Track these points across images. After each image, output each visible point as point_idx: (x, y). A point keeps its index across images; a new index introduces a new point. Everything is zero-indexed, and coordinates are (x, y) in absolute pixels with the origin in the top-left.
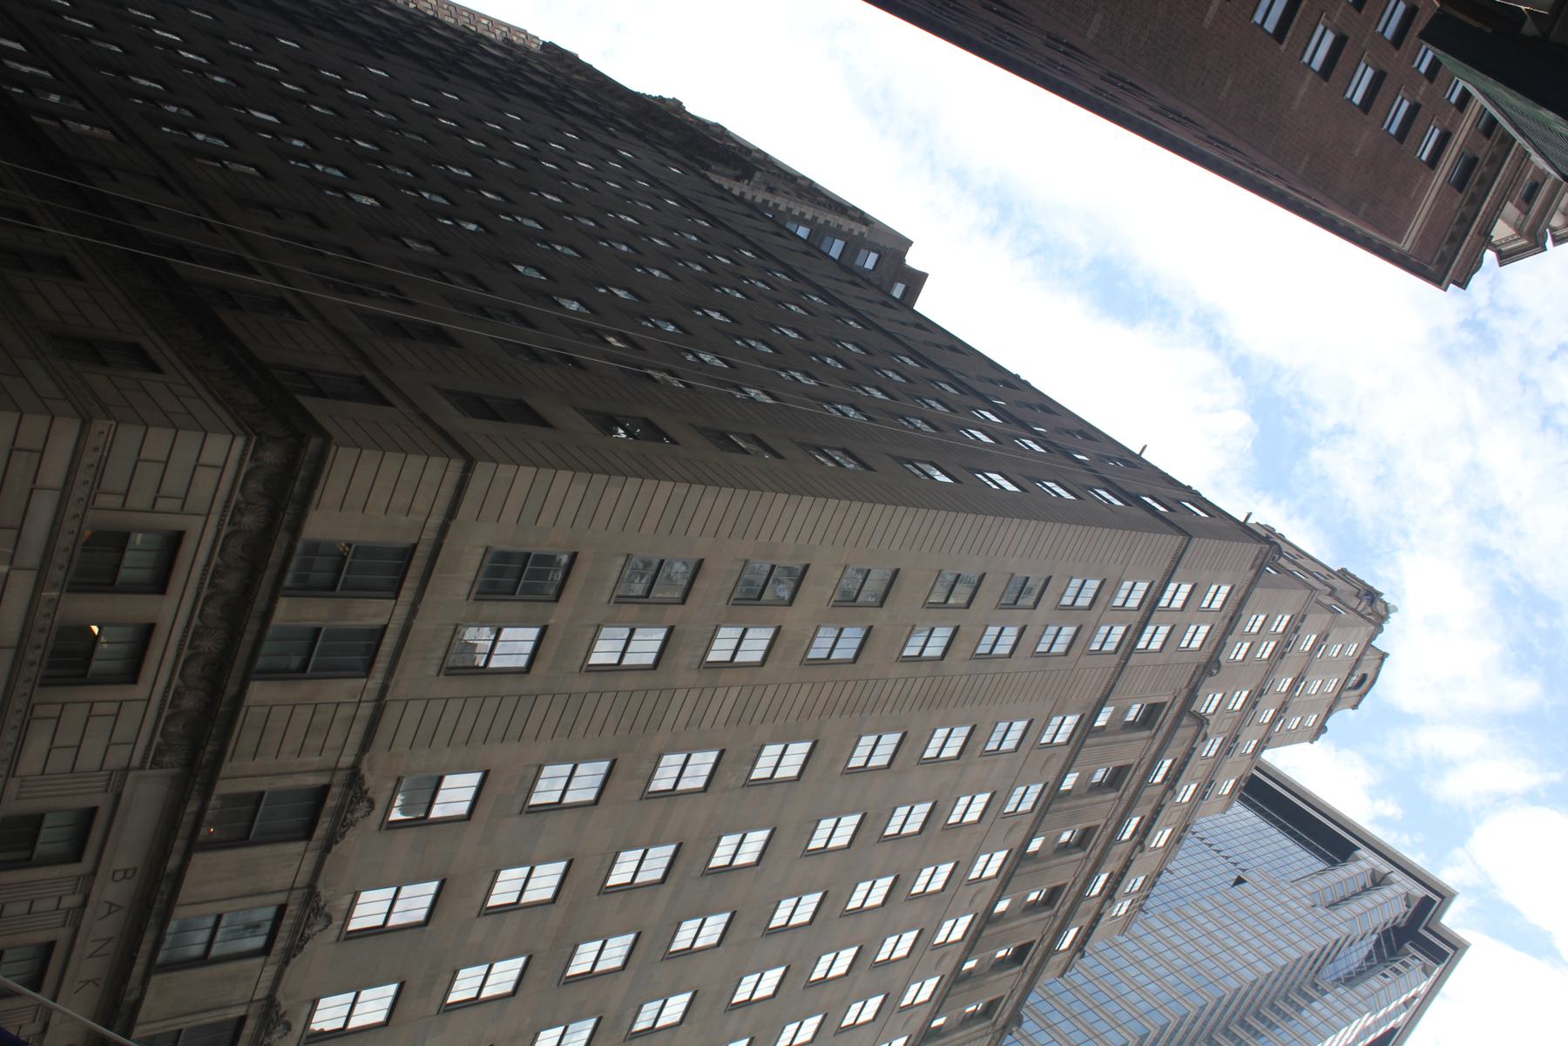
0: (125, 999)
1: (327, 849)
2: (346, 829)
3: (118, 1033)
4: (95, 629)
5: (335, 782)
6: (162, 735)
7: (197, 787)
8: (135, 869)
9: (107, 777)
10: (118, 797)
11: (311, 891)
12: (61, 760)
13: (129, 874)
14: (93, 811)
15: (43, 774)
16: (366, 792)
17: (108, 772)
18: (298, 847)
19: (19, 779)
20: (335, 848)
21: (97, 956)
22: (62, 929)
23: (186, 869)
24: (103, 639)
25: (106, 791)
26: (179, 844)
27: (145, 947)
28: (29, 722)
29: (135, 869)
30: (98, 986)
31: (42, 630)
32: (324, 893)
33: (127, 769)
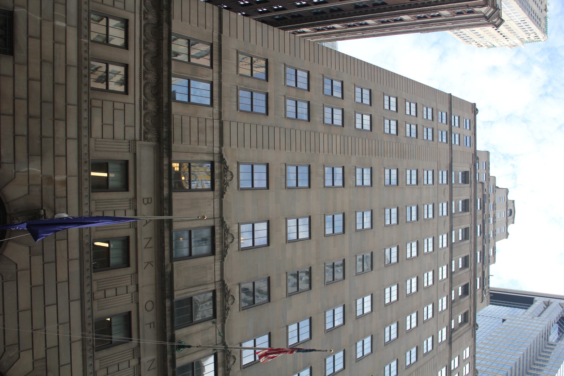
0: (166, 270)
1: (224, 321)
2: (229, 371)
4: (109, 319)
6: (144, 125)
7: (165, 151)
10: (135, 154)
12: (108, 131)
14: (130, 313)
16: (229, 292)
18: (212, 258)
20: (225, 196)
22: (130, 229)
23: (172, 196)
24: (113, 324)
27: (167, 253)
28: (91, 108)
29: (154, 323)
31: (86, 162)
33: (135, 140)
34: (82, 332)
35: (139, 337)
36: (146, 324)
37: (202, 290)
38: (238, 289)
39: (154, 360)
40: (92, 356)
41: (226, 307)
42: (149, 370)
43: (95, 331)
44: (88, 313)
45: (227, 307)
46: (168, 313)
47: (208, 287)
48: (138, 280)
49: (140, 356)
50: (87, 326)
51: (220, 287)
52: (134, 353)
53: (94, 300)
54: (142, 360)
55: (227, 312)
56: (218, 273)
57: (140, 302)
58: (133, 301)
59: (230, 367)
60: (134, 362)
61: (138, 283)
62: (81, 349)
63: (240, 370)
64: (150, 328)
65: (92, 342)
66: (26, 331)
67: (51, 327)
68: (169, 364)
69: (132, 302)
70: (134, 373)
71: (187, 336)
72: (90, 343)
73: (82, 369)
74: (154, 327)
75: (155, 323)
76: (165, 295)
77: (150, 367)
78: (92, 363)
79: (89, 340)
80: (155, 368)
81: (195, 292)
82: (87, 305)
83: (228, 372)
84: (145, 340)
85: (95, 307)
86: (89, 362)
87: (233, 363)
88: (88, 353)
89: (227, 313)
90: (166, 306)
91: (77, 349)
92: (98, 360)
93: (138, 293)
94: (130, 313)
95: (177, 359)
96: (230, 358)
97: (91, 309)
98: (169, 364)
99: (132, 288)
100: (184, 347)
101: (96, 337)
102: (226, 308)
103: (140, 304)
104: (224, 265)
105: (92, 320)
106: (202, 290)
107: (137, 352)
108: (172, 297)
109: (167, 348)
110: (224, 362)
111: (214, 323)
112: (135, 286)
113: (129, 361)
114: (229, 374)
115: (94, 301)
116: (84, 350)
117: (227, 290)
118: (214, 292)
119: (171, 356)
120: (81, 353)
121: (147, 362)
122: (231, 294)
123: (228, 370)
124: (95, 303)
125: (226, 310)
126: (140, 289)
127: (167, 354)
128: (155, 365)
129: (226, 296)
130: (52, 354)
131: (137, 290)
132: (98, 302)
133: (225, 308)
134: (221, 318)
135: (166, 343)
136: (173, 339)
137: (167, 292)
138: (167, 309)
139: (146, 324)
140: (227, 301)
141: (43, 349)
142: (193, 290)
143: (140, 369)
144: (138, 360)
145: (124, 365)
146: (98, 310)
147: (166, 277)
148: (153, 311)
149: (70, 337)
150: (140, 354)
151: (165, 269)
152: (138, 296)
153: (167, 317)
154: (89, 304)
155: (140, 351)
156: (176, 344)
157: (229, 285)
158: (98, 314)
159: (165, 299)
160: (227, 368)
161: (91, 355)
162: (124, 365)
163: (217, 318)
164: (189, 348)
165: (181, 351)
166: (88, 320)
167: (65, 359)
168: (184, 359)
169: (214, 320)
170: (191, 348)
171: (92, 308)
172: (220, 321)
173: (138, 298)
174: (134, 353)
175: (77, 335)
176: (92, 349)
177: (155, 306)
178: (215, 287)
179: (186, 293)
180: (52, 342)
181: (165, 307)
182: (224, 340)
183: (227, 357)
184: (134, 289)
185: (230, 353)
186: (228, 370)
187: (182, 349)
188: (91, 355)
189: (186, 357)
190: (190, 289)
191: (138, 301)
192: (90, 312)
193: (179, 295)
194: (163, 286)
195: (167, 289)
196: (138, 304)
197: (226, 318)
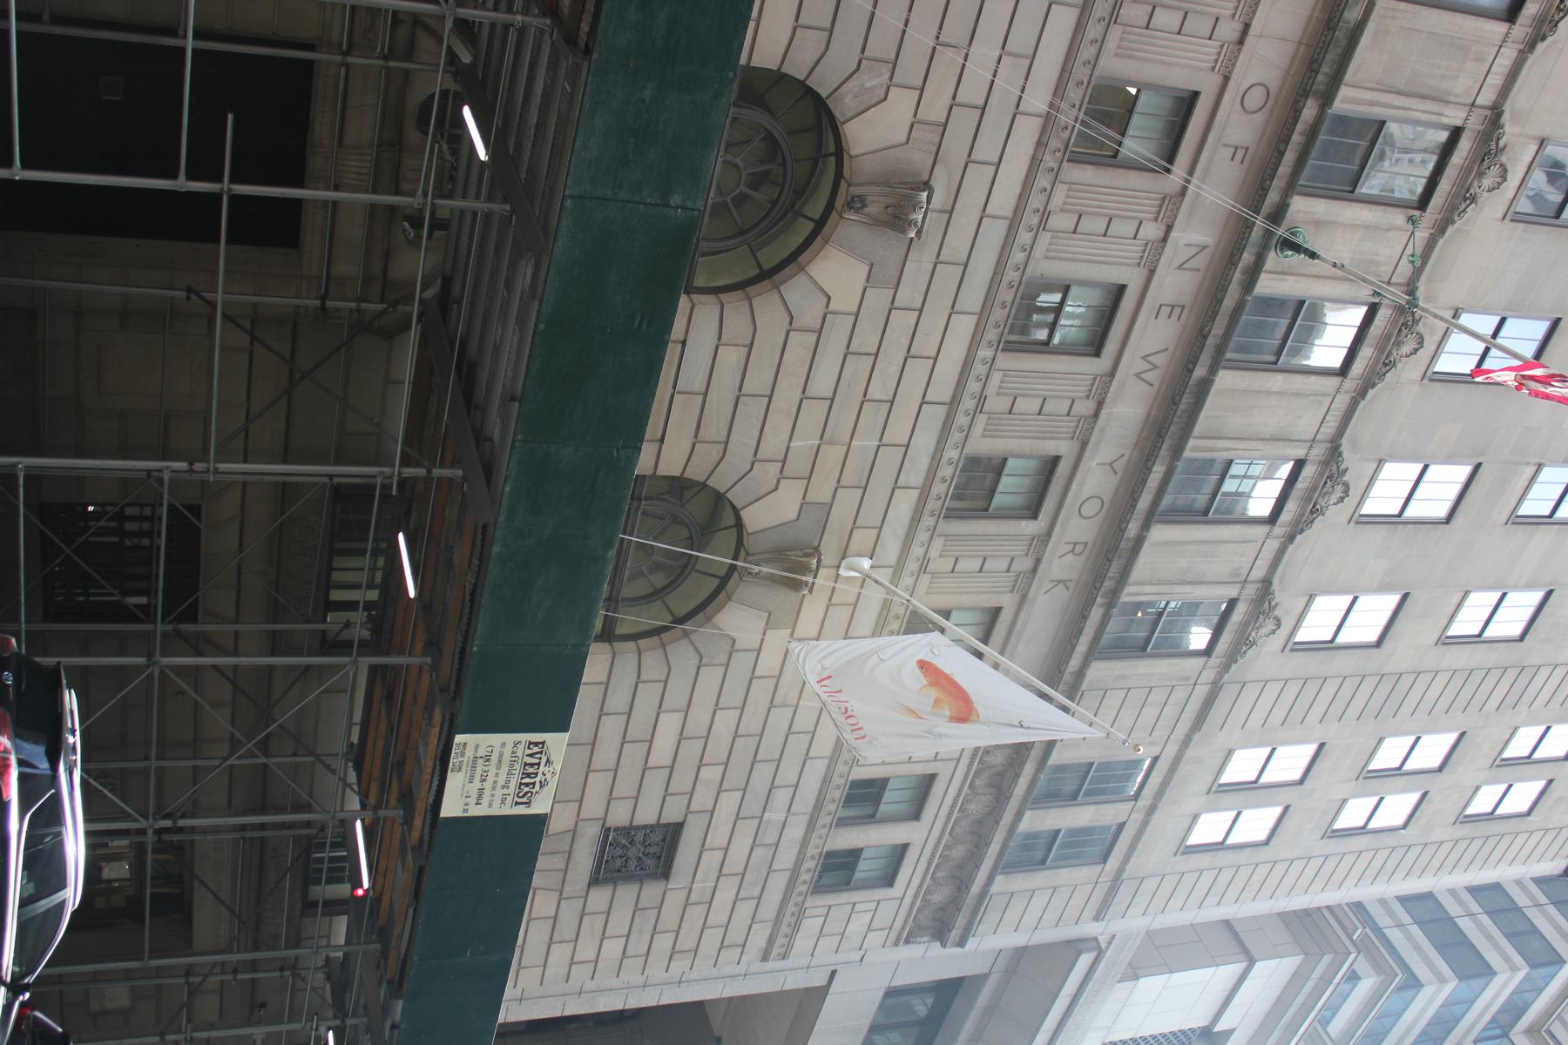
1: (1441, 228)
2: (1388, 368)
3: (1062, 693)
4: (1133, 91)
5: (1243, 597)
8: (1247, 149)
9: (1074, 424)
11: (1334, 452)
13: (1079, 548)
14: (1195, 95)
15: (952, 572)
17: (1144, 242)
19: (987, 415)
21: (1186, 269)
24: (1138, 108)
25: (1073, 438)
26: (1082, 646)
29: (1247, 149)
30: (1068, 589)
32: (1280, 596)
34: (1054, 96)
35: (1191, 172)
36: (1225, 145)
37: (1423, 112)
38: (1533, 153)
39: (1205, 247)
40: (1056, 169)
41: (1468, 190)
42: (1180, 267)
43: (1086, 109)
44: (1087, 52)
45: (1472, 191)
46: (1297, 138)
47: (1446, 113)
48: (1254, 12)
49: (1173, 222)
50: (1071, 85)
51: (1481, 128)
52: (1161, 206)
53: (1115, 23)
54: (1172, 235)
55: (1463, 206)
56: (1495, 80)
57: (1234, 77)
58: (1217, 68)
59: (1397, 360)
60: (1152, 231)
61: (1251, 19)
62: (1035, 138)
63: (1419, 379)
64: (1232, 160)
65: (1068, 132)
66: (920, 39)
67: (984, 52)
68: (1237, 276)
69: (1213, 68)
70: (1141, 257)
71: (1318, 224)
72: (1062, 134)
73: (1018, 191)
74: (1242, 163)
75: (1250, 150)
76: (1312, 85)
77: (1185, 263)
78: (1049, 188)
79: (1063, 124)
80: (1199, 270)
81: (1401, 111)
82: (1093, 31)
83: (1384, 370)
84: (1203, 186)
85: (1111, 43)
86: (1043, 181)
87: (1409, 353)
88: (1047, 157)
89: (1461, 209)
90: (1299, 116)
91: (1027, 131)
92: (1066, 187)
93: (1239, 51)
94: (1195, 95)
95: (1267, 272)
96: (1406, 336)
97: (1098, 44)
98: (1237, 276)
99: (1229, 31)
100: (1297, 248)
101: (1083, 123)
102: (1468, 195)
103: (1232, 84)
104: (1526, 67)
105: (1091, 75)
106: (1423, 112)
107: (1169, 209)
108: (1328, 97)
109: (1253, 234)
110: (1385, 338)
111: (1410, 219)
112: (1239, 27)
113: (1141, 222)
114: (1384, 375)
115: (1116, 26)
116: (1040, 144)
117: (1497, 143)
118: (1456, 133)
119: (1253, 258)
120: (1031, 151)
121: (1185, 245)
122: (1503, 159)
123: (1385, 364)
124: (1115, 33)
125: (1465, 199)
126: (1249, 39)
127: (1244, 249)
128: (1201, 261)
129: (1483, 160)
130: (963, 123)
131: (1241, 42)
132: (1123, 32)
133: (1463, 192)
134: (1439, 217)
135: (1256, 219)
136: (1277, 215)
137: (1320, 78)
138: (1300, 127)
139: (1225, 145)
140: (1481, 175)
141: (946, 100)
142: (1396, 103)
143: (1160, 254)
144: (1164, 229)
145: (1124, 228)
146: (1116, 55)
147: (1337, 33)
148: (1260, 118)
149: (1021, 97)
150: (1176, 216)
151: (1344, 9)
152: (1236, 58)
153: (1289, 147)
154: (1100, 28)
155: (1178, 209)
156: (1280, 232)
157: (1510, 129)
158: (1112, 65)
159: (1306, 98)
160: (1386, 358)
161: (1054, 165)
162: (1124, 228)
163: (1428, 211)
164: (1312, 260)
165: (1286, 257)
166: (1081, 72)
167: (987, 149)
168: (1282, 280)
169: (1417, 213)
170: (1316, 261)
171: (1101, 43)
172: (1433, 222)
173: (1234, 65)
174: (1161, 206)
175: (1037, 100)
176: (1062, 152)
177: (1269, 105)
178: (1467, 119)
179: (1372, 103)
180: (972, 92)
181: (1296, 120)
182: (1418, 280)
183: (1400, 330)
184: (1235, 36)
185: (1416, 322)
186: (1385, 364)
187: (1290, 253)
188: (1054, 165)
189: (1292, 278)
190: (1391, 96)
191: (1231, 72)
192: (1094, 50)
193: (1351, 103)
194: (1316, 56)
195: (1325, 69)
196: (1227, 79)
197: (1453, 222)
